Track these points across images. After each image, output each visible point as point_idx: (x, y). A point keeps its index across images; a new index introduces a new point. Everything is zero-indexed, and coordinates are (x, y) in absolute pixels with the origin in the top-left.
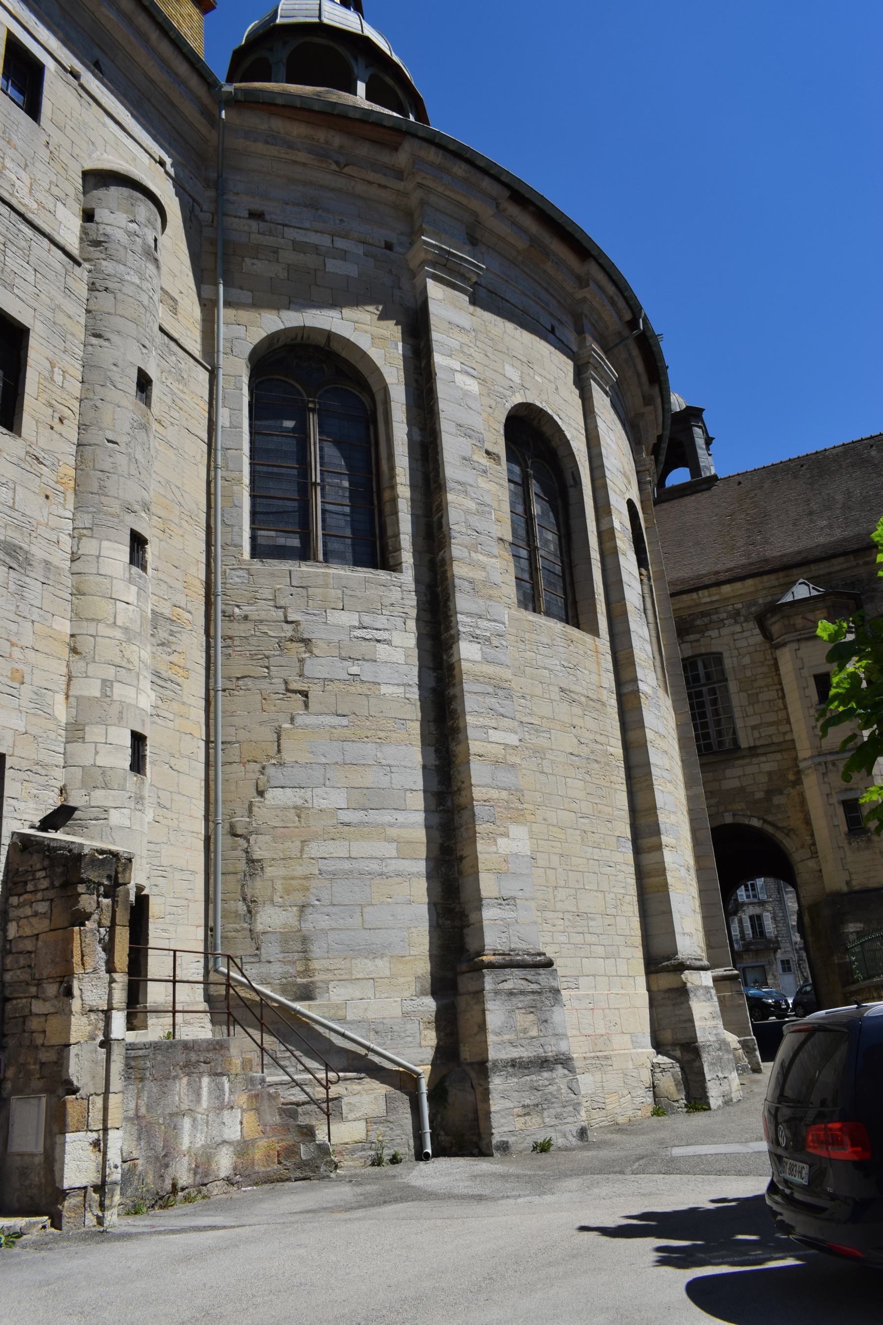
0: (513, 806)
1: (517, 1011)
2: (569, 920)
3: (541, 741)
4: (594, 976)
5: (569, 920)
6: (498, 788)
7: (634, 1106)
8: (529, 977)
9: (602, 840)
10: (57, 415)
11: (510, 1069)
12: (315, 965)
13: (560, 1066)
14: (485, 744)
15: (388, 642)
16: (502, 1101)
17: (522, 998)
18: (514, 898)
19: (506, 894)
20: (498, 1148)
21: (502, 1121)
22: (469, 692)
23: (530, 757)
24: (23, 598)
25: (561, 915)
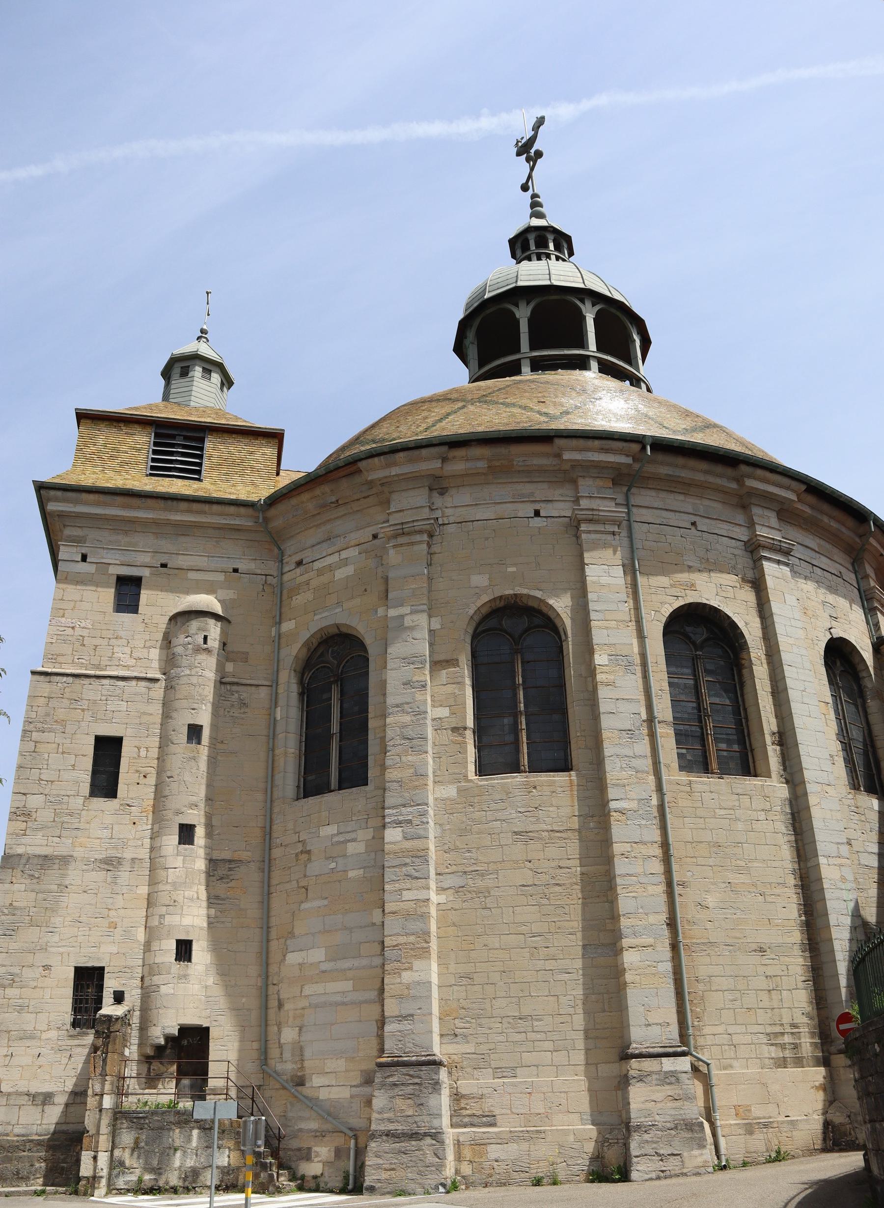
0: (418, 946)
1: (397, 1097)
2: (509, 1023)
3: (489, 882)
4: (537, 1066)
5: (509, 1023)
6: (407, 934)
7: (569, 1172)
8: (412, 1073)
9: (560, 952)
10: (142, 775)
11: (384, 1138)
12: (307, 1064)
13: (429, 1138)
14: (398, 903)
15: (354, 840)
16: (375, 1159)
17: (403, 1088)
18: (412, 1015)
19: (404, 1012)
20: (367, 1189)
21: (373, 1171)
22: (389, 867)
23: (472, 898)
24: (116, 883)
25: (499, 1020)
